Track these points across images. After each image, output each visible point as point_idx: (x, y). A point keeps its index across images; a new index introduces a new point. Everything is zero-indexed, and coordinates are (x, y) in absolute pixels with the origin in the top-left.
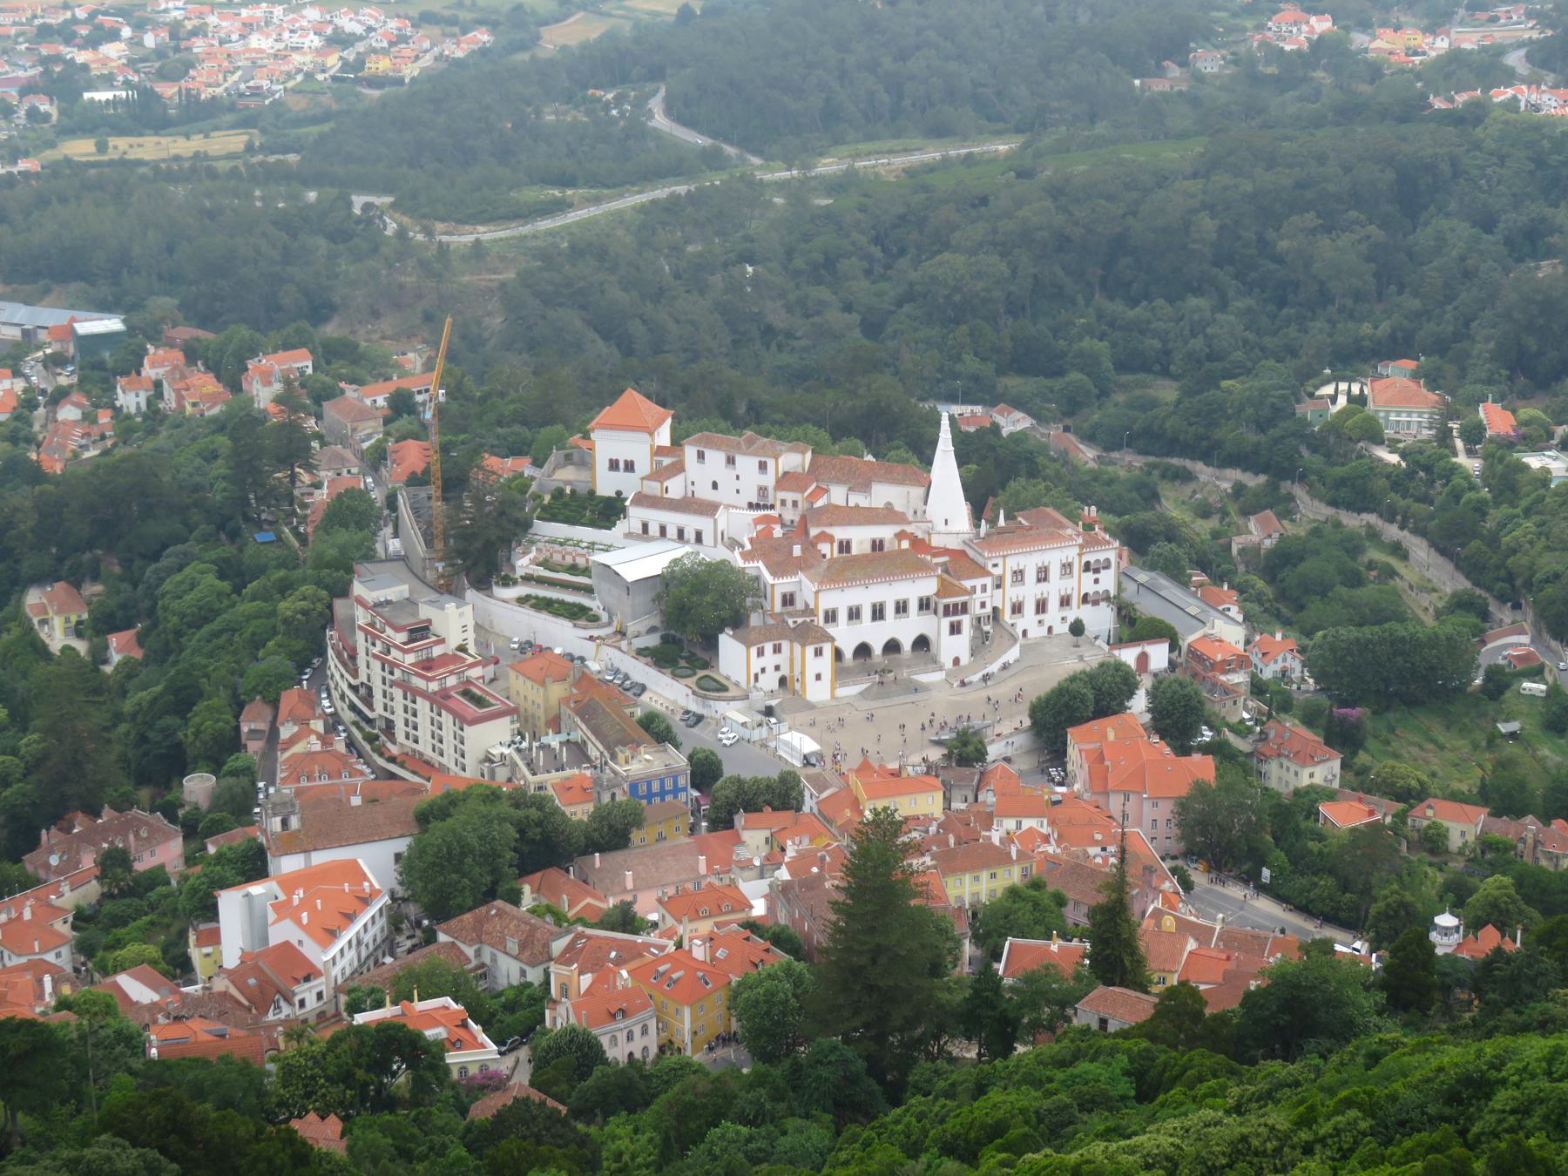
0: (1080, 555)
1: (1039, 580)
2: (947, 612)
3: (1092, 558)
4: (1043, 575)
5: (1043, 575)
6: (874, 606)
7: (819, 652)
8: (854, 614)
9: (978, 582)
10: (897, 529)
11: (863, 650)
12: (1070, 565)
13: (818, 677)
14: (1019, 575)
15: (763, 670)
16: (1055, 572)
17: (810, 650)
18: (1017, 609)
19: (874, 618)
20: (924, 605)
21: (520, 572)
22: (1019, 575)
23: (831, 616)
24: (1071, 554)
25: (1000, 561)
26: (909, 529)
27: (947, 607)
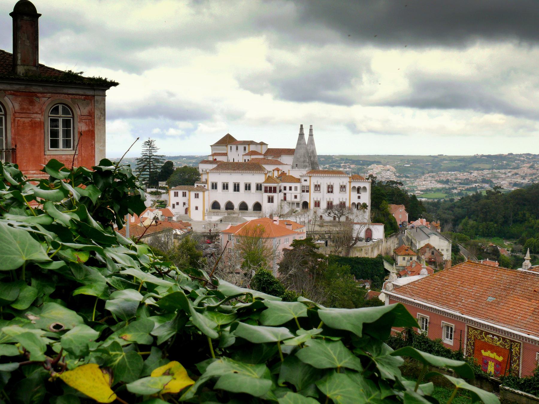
0: (350, 182)
1: (329, 192)
2: (266, 191)
3: (357, 185)
4: (330, 189)
5: (330, 189)
6: (235, 184)
7: (197, 196)
8: (225, 187)
9: (293, 185)
11: (229, 206)
12: (345, 187)
13: (197, 208)
14: (317, 187)
15: (178, 204)
16: (336, 189)
17: (193, 194)
18: (317, 204)
19: (235, 190)
20: (259, 187)
22: (317, 187)
23: (214, 186)
24: (345, 181)
25: (308, 179)
26: (280, 167)
27: (266, 188)
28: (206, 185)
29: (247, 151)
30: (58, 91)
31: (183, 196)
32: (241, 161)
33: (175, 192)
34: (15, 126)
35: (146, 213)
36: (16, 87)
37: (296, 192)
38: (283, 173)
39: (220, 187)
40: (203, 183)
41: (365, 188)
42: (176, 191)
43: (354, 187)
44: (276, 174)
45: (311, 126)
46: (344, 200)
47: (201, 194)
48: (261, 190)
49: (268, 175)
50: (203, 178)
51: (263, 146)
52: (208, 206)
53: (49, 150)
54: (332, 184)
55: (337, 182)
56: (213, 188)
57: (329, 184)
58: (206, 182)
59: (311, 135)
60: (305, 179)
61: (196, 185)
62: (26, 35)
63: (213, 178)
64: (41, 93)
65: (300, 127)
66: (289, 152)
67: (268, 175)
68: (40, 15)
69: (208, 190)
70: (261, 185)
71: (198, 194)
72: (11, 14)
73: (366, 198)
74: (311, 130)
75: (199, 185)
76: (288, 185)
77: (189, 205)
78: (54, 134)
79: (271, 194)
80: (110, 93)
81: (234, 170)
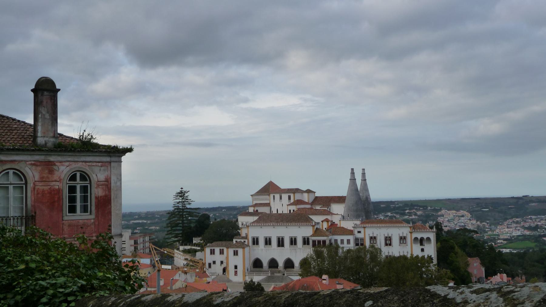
0: (411, 233)
1: (386, 245)
3: (419, 236)
4: (388, 241)
6: (279, 239)
7: (236, 253)
9: (345, 238)
10: (324, 217)
11: (273, 263)
12: (405, 238)
15: (214, 262)
16: (395, 241)
17: (231, 251)
20: (306, 241)
21: (194, 242)
23: (256, 241)
24: (405, 231)
25: (362, 230)
27: (314, 242)
28: (246, 241)
29: (292, 201)
30: (76, 160)
31: (221, 253)
32: (286, 211)
33: (211, 250)
34: (34, 194)
35: (178, 275)
36: (37, 158)
37: (349, 246)
38: (333, 224)
39: (262, 242)
40: (243, 238)
41: (428, 239)
42: (212, 248)
43: (416, 239)
44: (325, 225)
45: (364, 170)
46: (406, 254)
47: (240, 251)
48: (308, 244)
49: (315, 227)
50: (243, 232)
51: (311, 194)
52: (249, 264)
53: (66, 216)
54: (390, 235)
55: (396, 232)
56: (254, 244)
57: (386, 235)
58: (246, 237)
59: (364, 180)
60: (359, 230)
61: (234, 241)
62: (46, 109)
63: (253, 232)
64: (61, 162)
65: (350, 171)
66: (340, 200)
67: (315, 227)
68: (59, 90)
69: (248, 246)
70: (308, 239)
71: (237, 251)
72: (32, 90)
73: (431, 250)
74: (364, 174)
75: (238, 240)
76: (339, 238)
77: (227, 264)
78: (72, 200)
79: (319, 249)
80: (126, 158)
81: (277, 222)
